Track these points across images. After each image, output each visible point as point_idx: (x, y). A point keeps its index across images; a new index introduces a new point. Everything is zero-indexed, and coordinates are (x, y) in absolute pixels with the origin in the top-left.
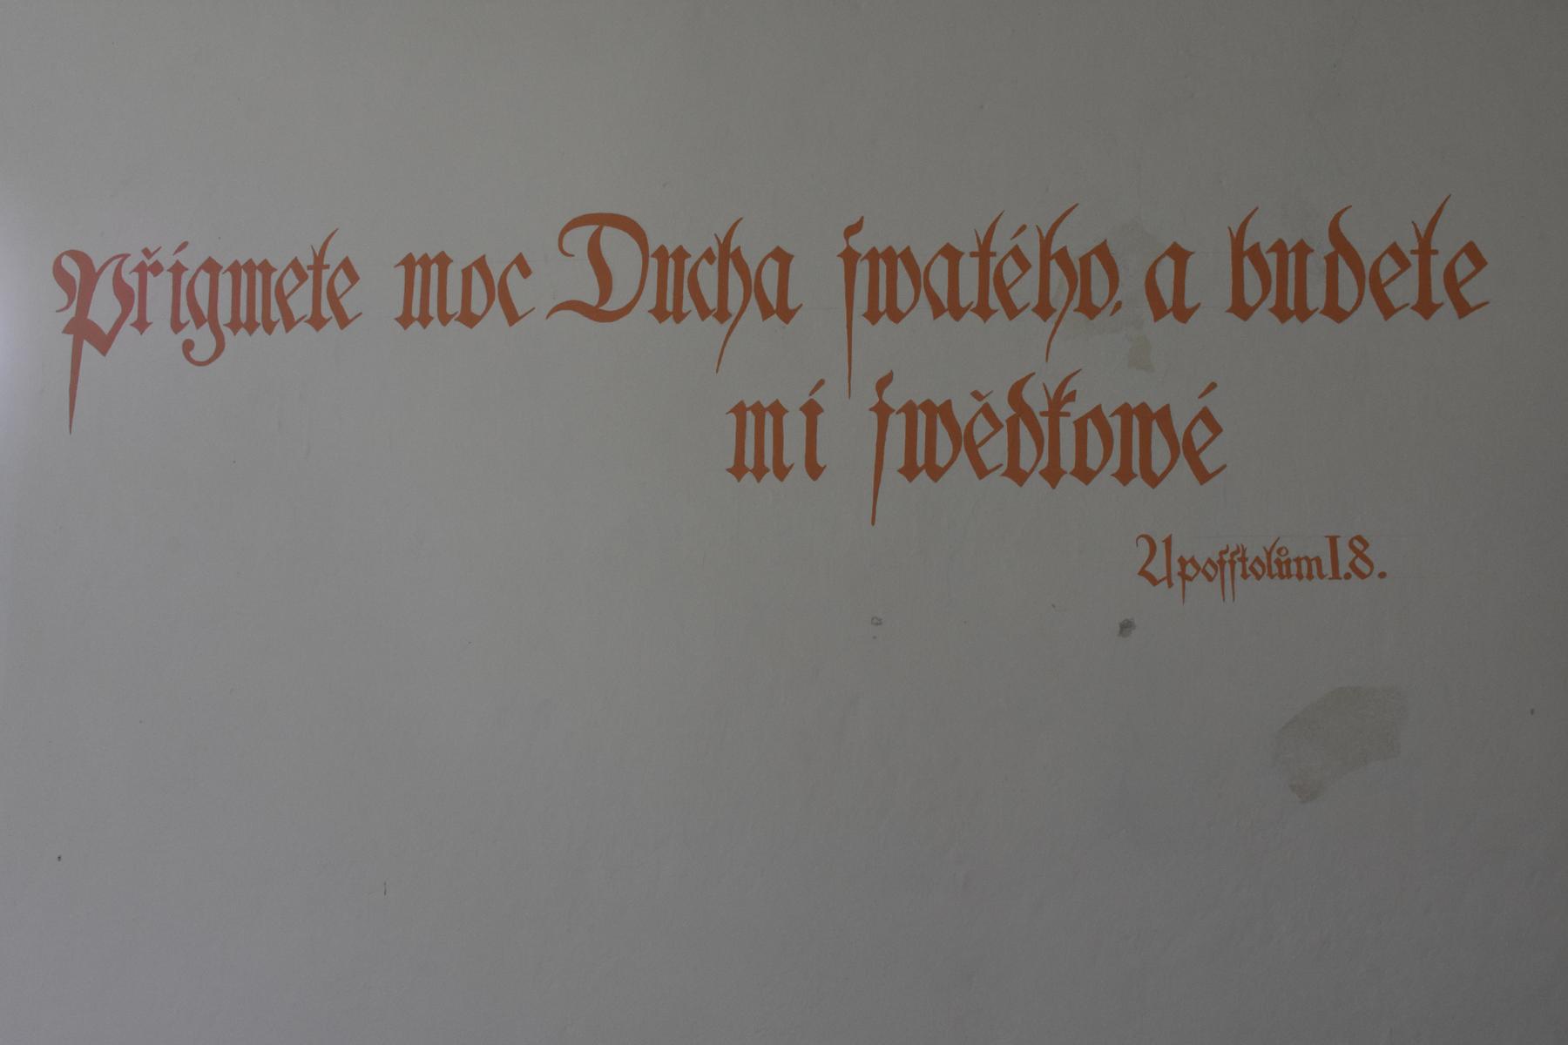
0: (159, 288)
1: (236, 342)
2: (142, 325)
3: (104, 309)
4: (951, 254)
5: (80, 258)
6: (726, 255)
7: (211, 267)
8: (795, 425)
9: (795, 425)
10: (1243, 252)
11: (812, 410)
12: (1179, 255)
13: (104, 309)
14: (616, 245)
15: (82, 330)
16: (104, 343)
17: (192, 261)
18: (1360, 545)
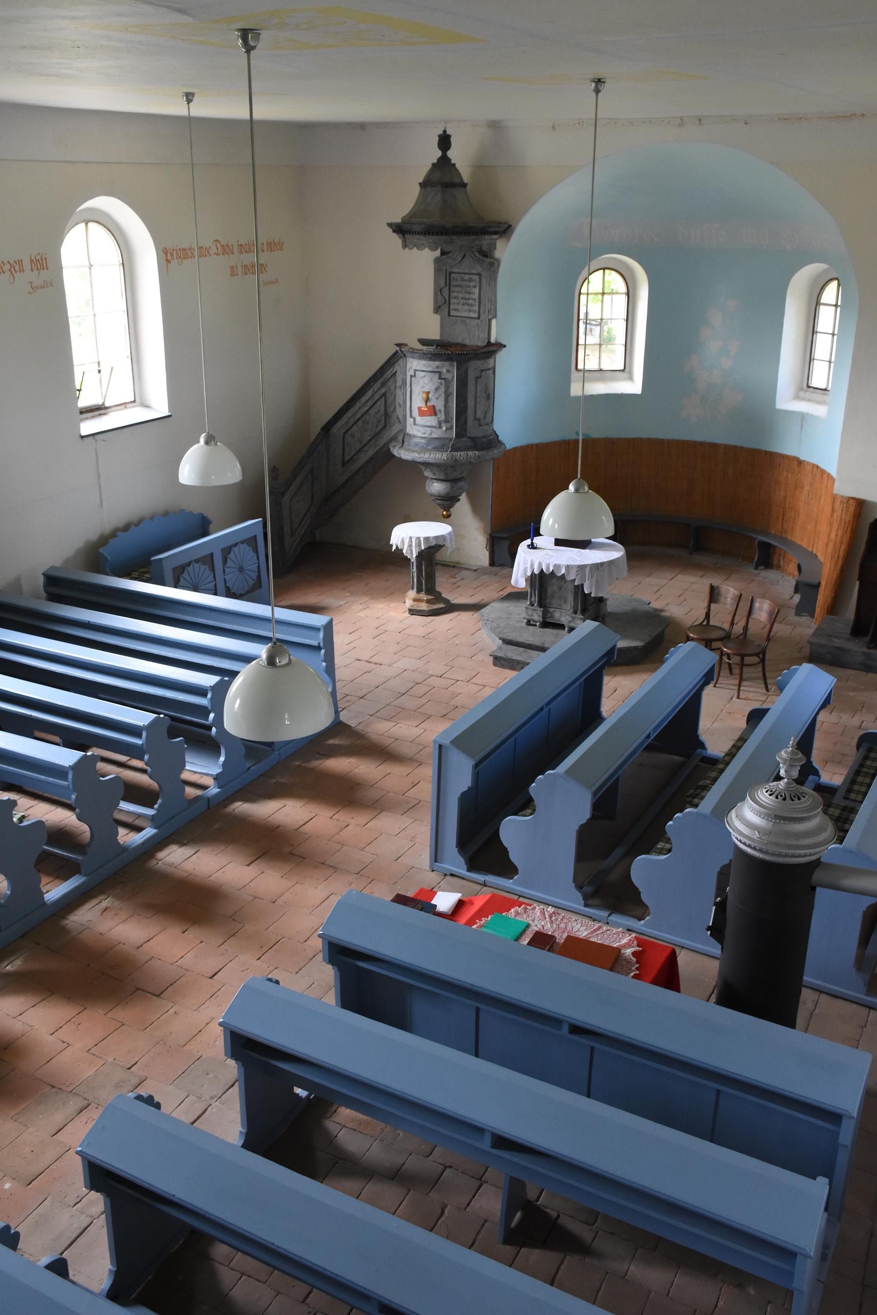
0: (175, 252)
1: (184, 261)
2: (173, 259)
3: (169, 257)
4: (246, 244)
5: (165, 248)
6: (228, 246)
7: (180, 249)
8: (235, 268)
9: (235, 268)
10: (267, 243)
11: (236, 267)
12: (263, 244)
13: (169, 257)
14: (218, 243)
15: (167, 260)
16: (170, 262)
17: (178, 248)
18: (277, 279)
